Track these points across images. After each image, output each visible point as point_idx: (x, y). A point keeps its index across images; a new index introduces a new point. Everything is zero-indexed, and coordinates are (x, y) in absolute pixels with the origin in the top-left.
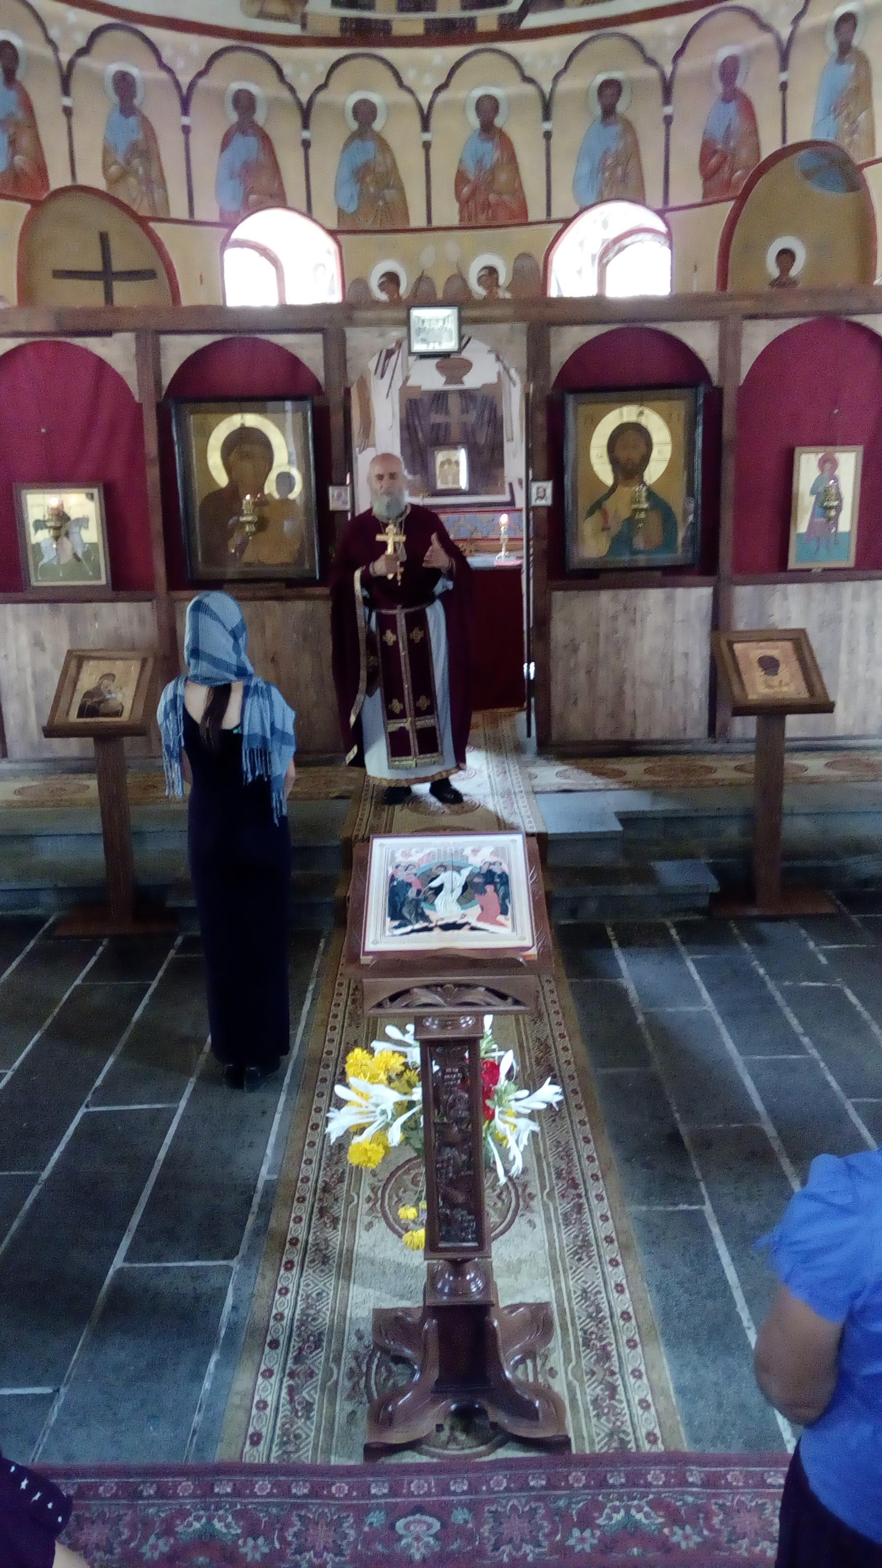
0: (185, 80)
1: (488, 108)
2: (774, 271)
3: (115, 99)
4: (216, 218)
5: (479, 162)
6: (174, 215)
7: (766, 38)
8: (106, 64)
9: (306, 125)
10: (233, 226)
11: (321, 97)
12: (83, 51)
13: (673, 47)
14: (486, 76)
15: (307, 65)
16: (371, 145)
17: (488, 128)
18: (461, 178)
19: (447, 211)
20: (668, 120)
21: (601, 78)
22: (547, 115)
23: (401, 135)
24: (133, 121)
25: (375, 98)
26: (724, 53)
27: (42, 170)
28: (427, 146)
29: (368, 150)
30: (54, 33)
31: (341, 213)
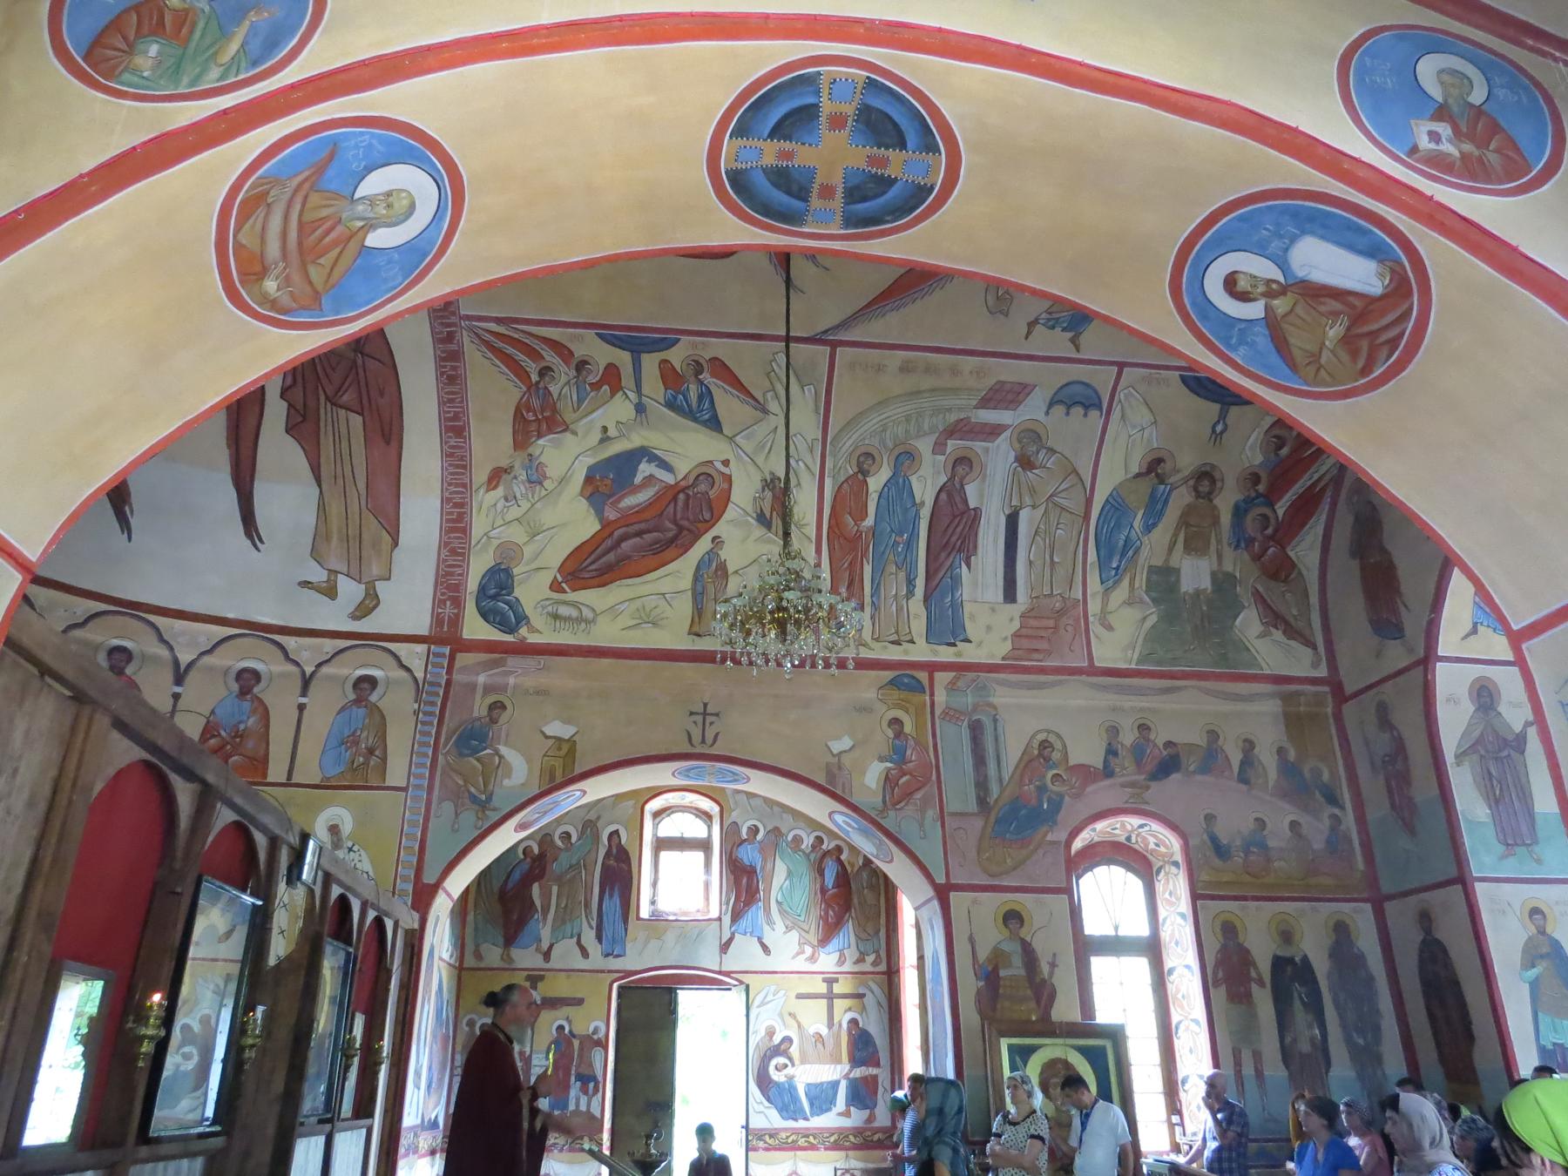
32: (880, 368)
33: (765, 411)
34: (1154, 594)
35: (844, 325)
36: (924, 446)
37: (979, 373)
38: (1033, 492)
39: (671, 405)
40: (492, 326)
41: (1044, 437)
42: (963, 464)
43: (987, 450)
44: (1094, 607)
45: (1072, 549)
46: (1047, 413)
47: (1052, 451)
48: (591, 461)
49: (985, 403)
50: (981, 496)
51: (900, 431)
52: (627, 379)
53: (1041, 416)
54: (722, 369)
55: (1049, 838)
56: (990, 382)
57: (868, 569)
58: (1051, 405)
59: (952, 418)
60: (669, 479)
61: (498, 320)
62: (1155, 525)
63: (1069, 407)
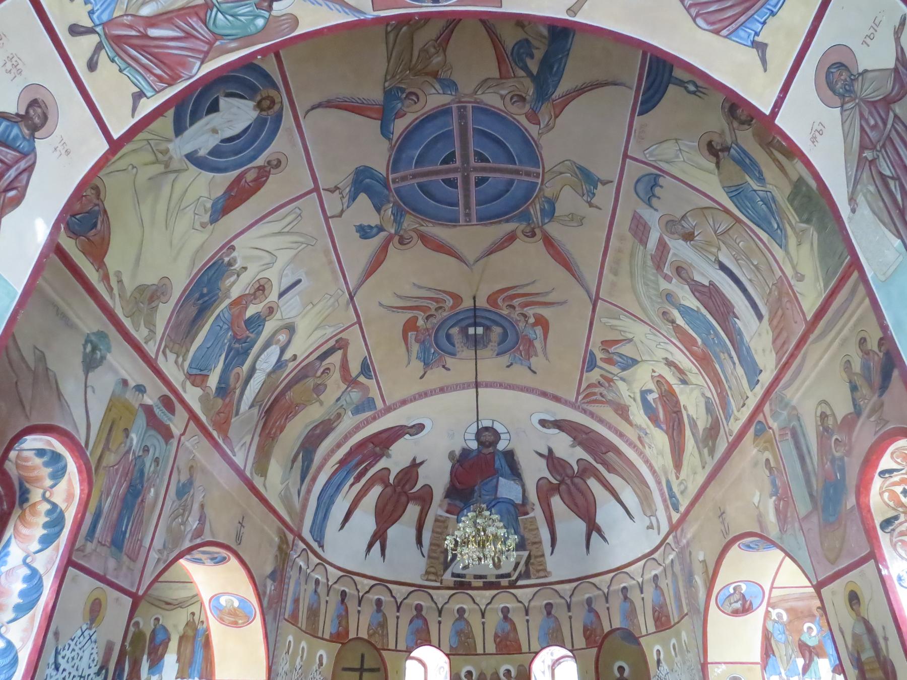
0: (399, 601)
1: (505, 611)
2: (618, 675)
3: (375, 607)
4: (404, 649)
5: (503, 630)
6: (390, 647)
7: (600, 592)
8: (373, 596)
9: (440, 616)
10: (411, 652)
11: (446, 606)
12: (367, 592)
13: (569, 593)
14: (504, 600)
15: (441, 596)
16: (463, 623)
17: (506, 618)
18: (496, 636)
19: (491, 647)
20: (570, 617)
21: (545, 602)
22: (527, 614)
23: (475, 621)
24: (380, 614)
25: (465, 607)
26: (587, 596)
27: (347, 633)
28: (483, 623)
29: (462, 624)
30: (359, 587)
31: (451, 647)
32: (613, 284)
33: (630, 340)
34: (805, 216)
35: (588, 292)
36: (664, 285)
37: (622, 238)
38: (709, 243)
39: (624, 369)
40: (580, 397)
41: (671, 218)
42: (679, 270)
43: (675, 254)
44: (789, 272)
45: (754, 247)
46: (656, 210)
47: (684, 217)
48: (642, 411)
49: (644, 242)
50: (703, 275)
51: (653, 292)
52: (610, 376)
53: (657, 215)
54: (607, 344)
55: (848, 507)
56: (629, 235)
57: (717, 366)
58: (651, 207)
59: (650, 263)
60: (655, 395)
61: (578, 394)
62: (760, 173)
63: (654, 195)
